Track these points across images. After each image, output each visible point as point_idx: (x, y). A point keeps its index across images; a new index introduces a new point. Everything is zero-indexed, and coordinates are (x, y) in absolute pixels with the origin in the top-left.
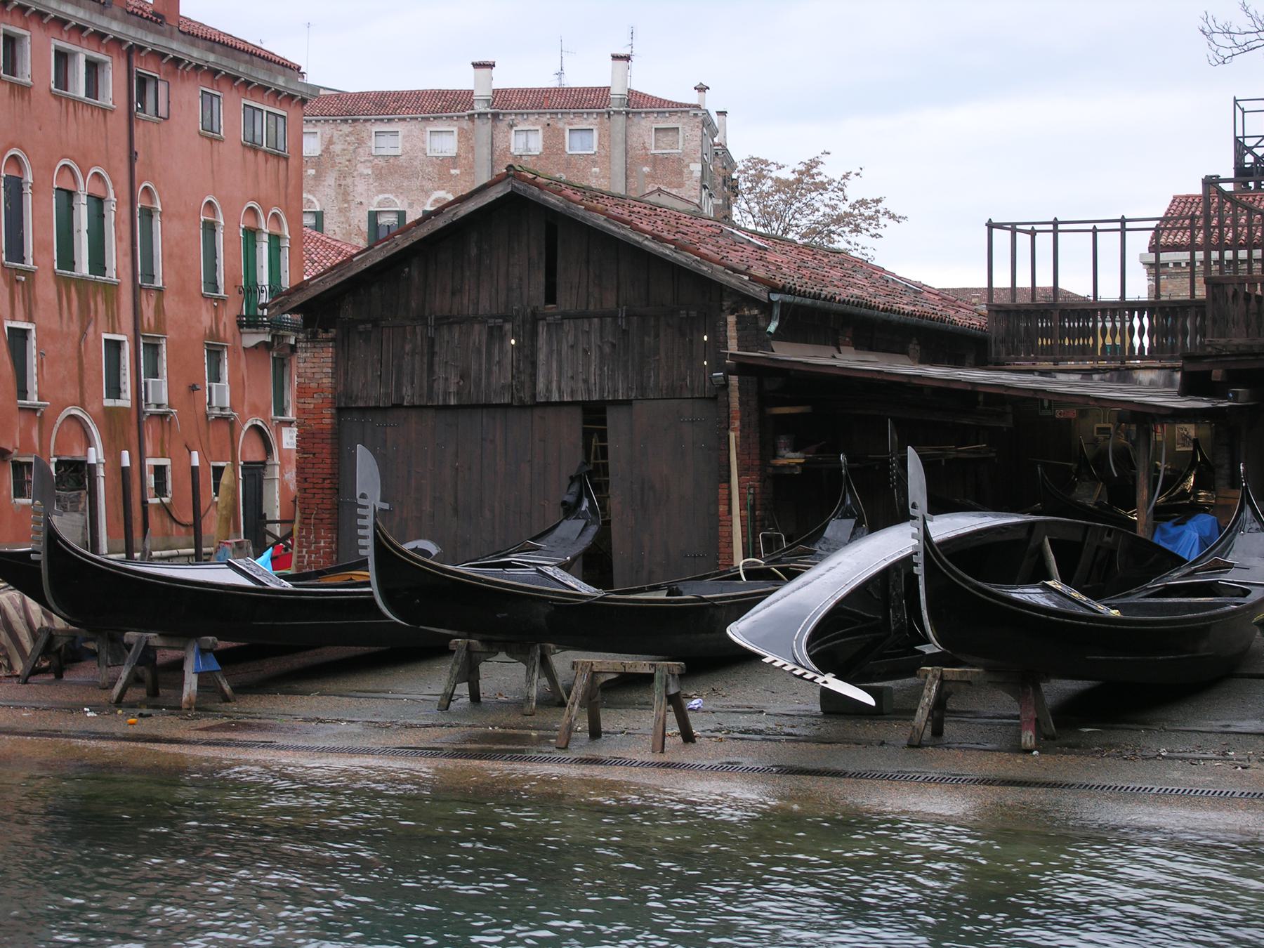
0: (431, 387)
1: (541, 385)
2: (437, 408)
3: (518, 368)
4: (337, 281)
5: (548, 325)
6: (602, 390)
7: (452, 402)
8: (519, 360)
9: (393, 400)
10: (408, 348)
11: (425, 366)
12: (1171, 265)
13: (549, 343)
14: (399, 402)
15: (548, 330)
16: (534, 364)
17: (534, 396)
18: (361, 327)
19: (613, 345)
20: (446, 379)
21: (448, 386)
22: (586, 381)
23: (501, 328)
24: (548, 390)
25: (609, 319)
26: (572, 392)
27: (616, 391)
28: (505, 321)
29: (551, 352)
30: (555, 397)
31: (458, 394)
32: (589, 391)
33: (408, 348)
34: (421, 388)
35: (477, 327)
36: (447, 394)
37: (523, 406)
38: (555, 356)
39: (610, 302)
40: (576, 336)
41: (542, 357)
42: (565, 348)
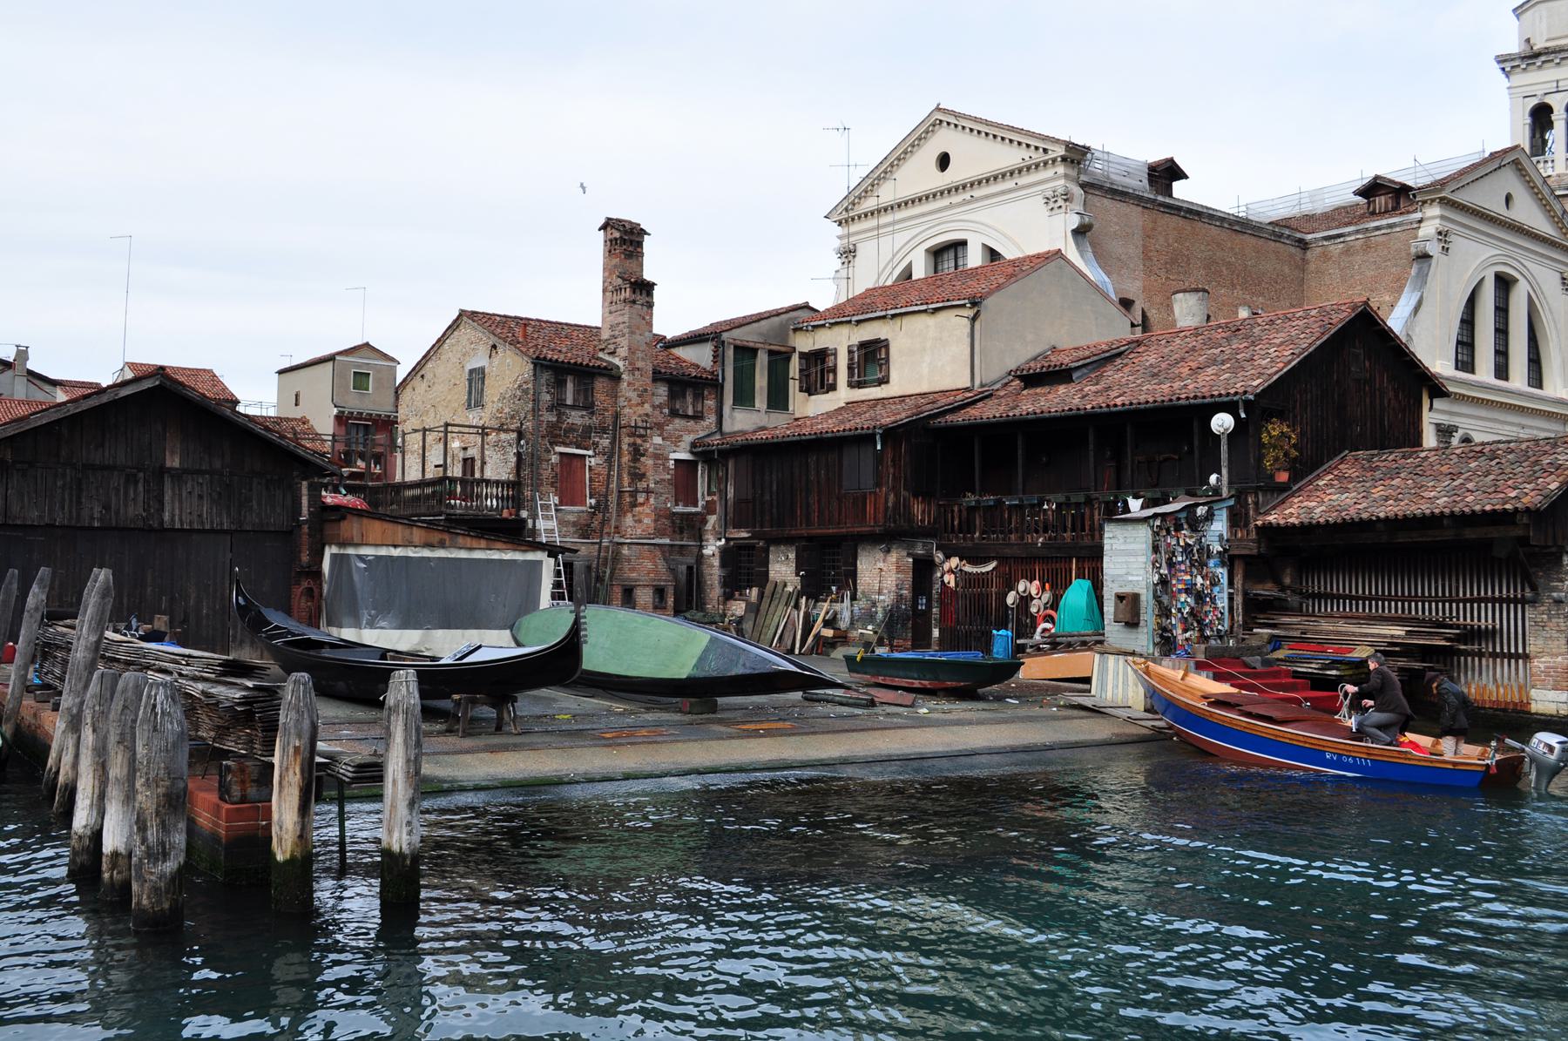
0: (78, 515)
1: (167, 516)
2: (83, 528)
3: (149, 504)
4: (17, 432)
5: (172, 477)
6: (212, 523)
7: (96, 524)
8: (149, 499)
9: (47, 520)
10: (59, 483)
11: (74, 499)
13: (173, 489)
14: (52, 522)
15: (172, 481)
16: (162, 503)
17: (162, 522)
18: (18, 466)
19: (220, 494)
20: (92, 509)
21: (93, 513)
22: (200, 516)
23: (135, 475)
24: (173, 520)
25: (217, 477)
26: (191, 523)
27: (222, 524)
28: (140, 471)
29: (174, 494)
30: (178, 526)
31: (100, 520)
32: (202, 523)
33: (59, 483)
34: (70, 512)
35: (116, 473)
36: (92, 518)
37: (151, 530)
38: (177, 497)
39: (217, 464)
40: (193, 486)
41: (167, 498)
42: (184, 494)
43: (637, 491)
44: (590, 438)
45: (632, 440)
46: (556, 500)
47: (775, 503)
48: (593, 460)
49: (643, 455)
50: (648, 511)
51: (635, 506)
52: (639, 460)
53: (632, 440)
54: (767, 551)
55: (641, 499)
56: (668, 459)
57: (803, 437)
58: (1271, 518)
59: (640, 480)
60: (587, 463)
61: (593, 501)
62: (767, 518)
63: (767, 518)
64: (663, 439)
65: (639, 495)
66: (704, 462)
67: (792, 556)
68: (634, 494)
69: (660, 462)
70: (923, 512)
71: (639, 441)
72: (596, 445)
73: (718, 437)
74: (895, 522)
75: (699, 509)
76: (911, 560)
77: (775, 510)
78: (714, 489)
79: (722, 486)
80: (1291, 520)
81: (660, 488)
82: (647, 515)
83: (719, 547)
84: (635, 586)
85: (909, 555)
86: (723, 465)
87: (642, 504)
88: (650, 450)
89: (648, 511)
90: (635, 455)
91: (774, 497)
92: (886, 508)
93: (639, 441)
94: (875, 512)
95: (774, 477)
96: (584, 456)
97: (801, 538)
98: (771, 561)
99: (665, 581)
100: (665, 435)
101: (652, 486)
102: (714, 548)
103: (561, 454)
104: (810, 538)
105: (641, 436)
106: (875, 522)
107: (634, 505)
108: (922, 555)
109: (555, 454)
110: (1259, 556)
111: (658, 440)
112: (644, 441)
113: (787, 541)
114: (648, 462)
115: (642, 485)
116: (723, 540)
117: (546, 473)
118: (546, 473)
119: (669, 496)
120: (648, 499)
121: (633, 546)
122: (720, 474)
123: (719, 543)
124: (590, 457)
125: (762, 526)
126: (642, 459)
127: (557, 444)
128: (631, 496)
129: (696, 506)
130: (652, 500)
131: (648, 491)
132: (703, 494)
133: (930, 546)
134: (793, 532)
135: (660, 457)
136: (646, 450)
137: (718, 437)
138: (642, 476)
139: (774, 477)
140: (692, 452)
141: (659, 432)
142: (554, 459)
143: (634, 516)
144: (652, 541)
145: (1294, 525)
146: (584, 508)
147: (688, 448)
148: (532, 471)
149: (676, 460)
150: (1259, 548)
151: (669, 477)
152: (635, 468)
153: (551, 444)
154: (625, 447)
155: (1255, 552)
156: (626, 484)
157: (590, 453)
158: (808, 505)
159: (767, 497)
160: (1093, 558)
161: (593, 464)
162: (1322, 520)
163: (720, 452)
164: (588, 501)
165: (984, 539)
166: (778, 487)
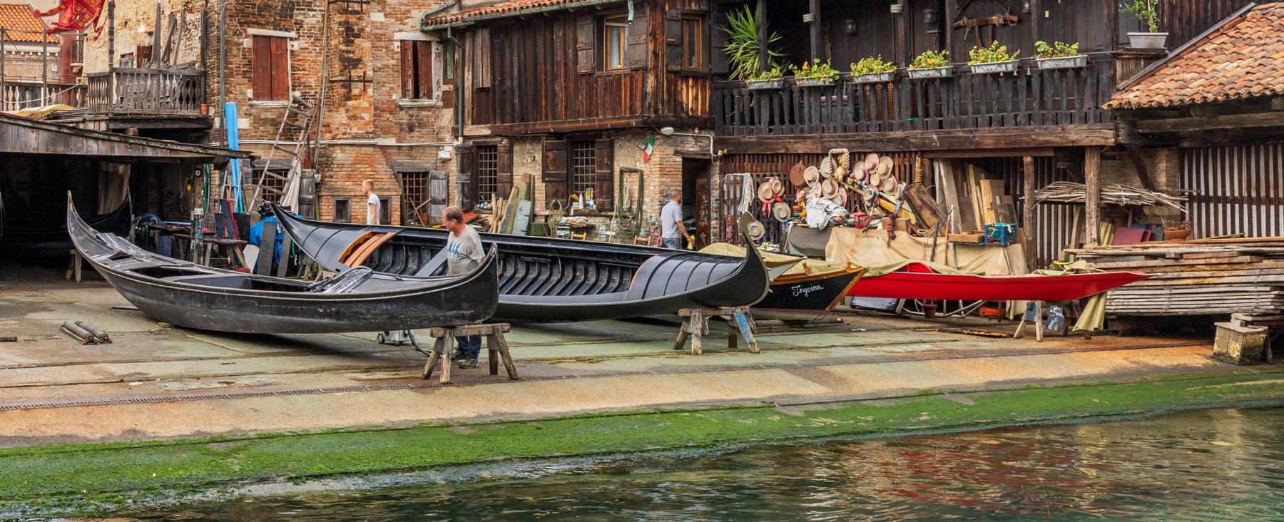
12: (13, 53)
43: (350, 80)
44: (291, 16)
45: (343, 18)
46: (250, 93)
47: (516, 90)
48: (295, 43)
49: (358, 36)
50: (366, 104)
51: (348, 98)
52: (353, 42)
53: (343, 18)
54: (510, 151)
55: (356, 91)
56: (391, 41)
57: (544, 9)
58: (1130, 96)
59: (355, 67)
60: (289, 48)
61: (298, 94)
62: (509, 110)
63: (509, 110)
64: (386, 15)
65: (353, 85)
66: (439, 43)
67: (539, 157)
68: (348, 83)
69: (382, 44)
70: (696, 98)
71: (353, 19)
72: (300, 24)
73: (455, 11)
74: (656, 111)
75: (432, 102)
76: (679, 159)
77: (516, 101)
78: (450, 75)
79: (459, 72)
80: (1157, 98)
81: (381, 76)
82: (365, 110)
83: (457, 148)
84: (350, 197)
85: (677, 153)
86: (459, 47)
87: (358, 97)
88: (368, 29)
89: (366, 104)
90: (348, 36)
91: (516, 83)
92: (645, 95)
93: (353, 19)
94: (631, 99)
95: (515, 59)
96: (286, 38)
97: (549, 135)
98: (515, 164)
99: (389, 190)
100: (388, 11)
101: (370, 73)
102: (451, 149)
103: (255, 36)
104: (558, 135)
105: (356, 12)
106: (631, 113)
107: (348, 97)
108: (696, 153)
109: (247, 37)
110: (1119, 147)
111: (378, 17)
112: (360, 19)
113: (535, 138)
114: (363, 44)
115: (356, 73)
116: (461, 139)
117: (236, 61)
118: (236, 61)
119: (395, 86)
120: (365, 90)
121: (347, 148)
122: (457, 56)
123: (456, 143)
124: (291, 39)
125: (503, 122)
126: (357, 41)
127: (249, 24)
128: (343, 86)
129: (430, 97)
130: (370, 91)
131: (364, 80)
132: (438, 83)
133: (705, 142)
134: (538, 127)
135: (380, 39)
136: (362, 30)
137: (455, 11)
138: (357, 63)
139: (515, 59)
140: (423, 31)
141: (379, 7)
142: (247, 43)
143: (347, 111)
144: (372, 142)
145: (1160, 105)
146: (286, 103)
147: (418, 26)
148: (218, 59)
149: (401, 41)
150: (1117, 136)
151: (394, 62)
152: (348, 52)
153: (241, 24)
154: (335, 27)
155: (1111, 141)
156: (337, 72)
157: (293, 34)
158: (554, 94)
159: (508, 83)
160: (905, 153)
161: (296, 48)
162: (1198, 99)
163: (455, 31)
164: (291, 94)
165: (770, 131)
166: (519, 70)
